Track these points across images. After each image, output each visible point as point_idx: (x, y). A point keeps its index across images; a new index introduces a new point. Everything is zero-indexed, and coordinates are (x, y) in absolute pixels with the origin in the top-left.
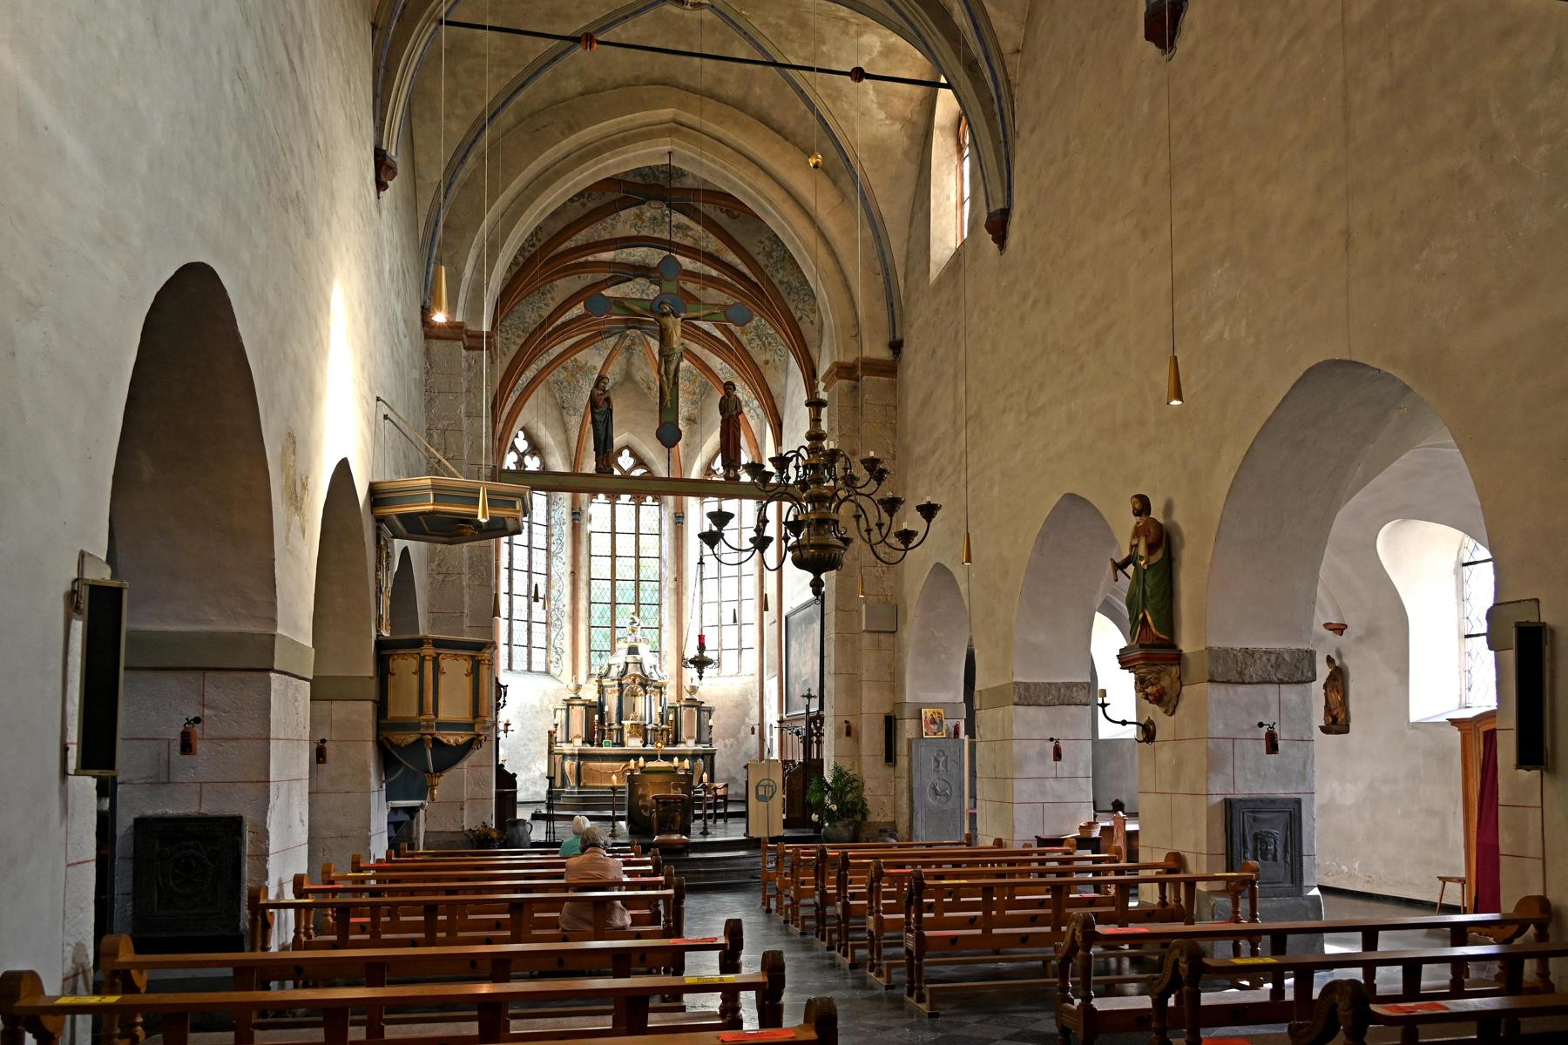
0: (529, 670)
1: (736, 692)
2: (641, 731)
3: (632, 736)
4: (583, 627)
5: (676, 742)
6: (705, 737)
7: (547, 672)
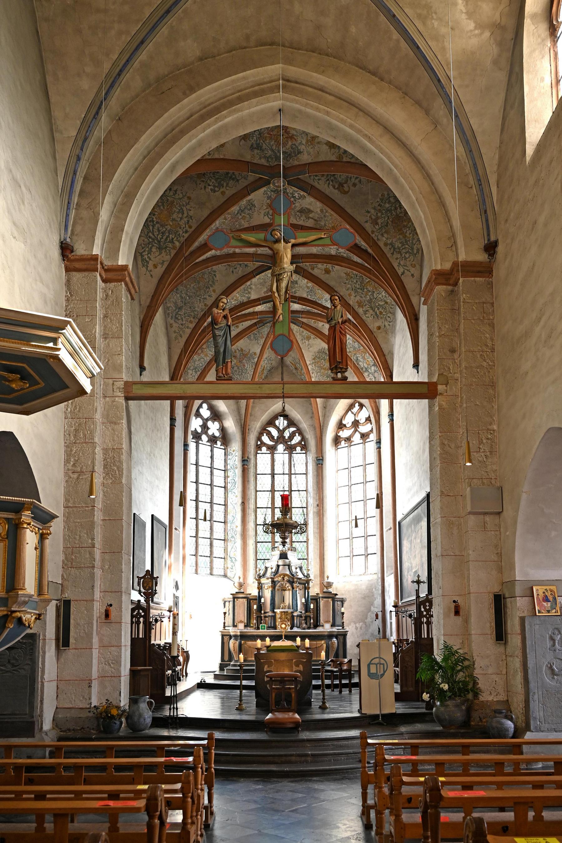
1: (364, 587)
4: (251, 543)
5: (316, 626)
6: (338, 621)
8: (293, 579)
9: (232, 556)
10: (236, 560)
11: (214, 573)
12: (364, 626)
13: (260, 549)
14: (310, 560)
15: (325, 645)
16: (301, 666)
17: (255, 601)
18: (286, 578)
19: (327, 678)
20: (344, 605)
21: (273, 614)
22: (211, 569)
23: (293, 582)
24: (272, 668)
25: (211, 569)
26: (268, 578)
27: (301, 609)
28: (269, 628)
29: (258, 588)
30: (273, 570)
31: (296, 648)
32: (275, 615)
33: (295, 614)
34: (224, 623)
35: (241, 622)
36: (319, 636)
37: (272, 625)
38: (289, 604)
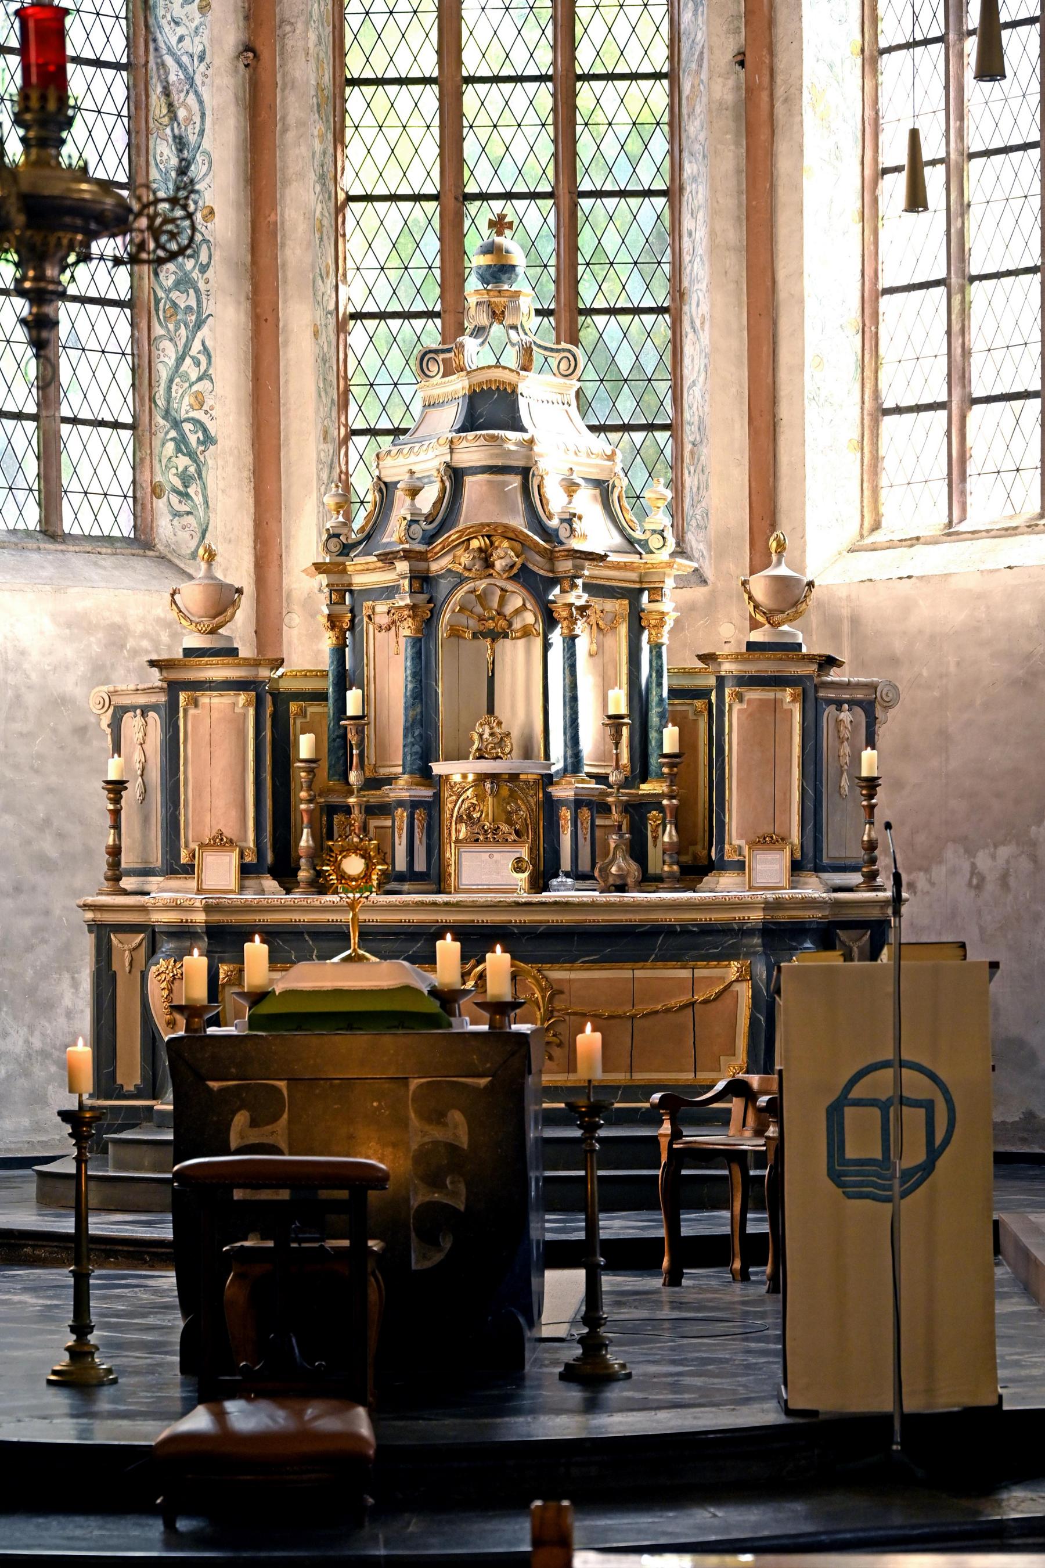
0: (50, 530)
2: (530, 811)
3: (484, 836)
4: (299, 320)
6: (844, 837)
7: (142, 541)
8: (551, 557)
9: (184, 408)
10: (208, 439)
11: (68, 525)
12: (1025, 864)
13: (371, 362)
14: (690, 434)
15: (745, 991)
16: (457, 1116)
17: (313, 709)
18: (504, 556)
19: (630, 1197)
20: (883, 732)
21: (426, 793)
22: (50, 494)
23: (553, 582)
24: (279, 1131)
25: (50, 494)
26: (388, 559)
27: (602, 757)
28: (391, 881)
29: (333, 621)
30: (426, 501)
31: (434, 1006)
32: (437, 796)
33: (564, 792)
34: (115, 852)
35: (220, 843)
36: (708, 930)
37: (420, 866)
38: (529, 724)
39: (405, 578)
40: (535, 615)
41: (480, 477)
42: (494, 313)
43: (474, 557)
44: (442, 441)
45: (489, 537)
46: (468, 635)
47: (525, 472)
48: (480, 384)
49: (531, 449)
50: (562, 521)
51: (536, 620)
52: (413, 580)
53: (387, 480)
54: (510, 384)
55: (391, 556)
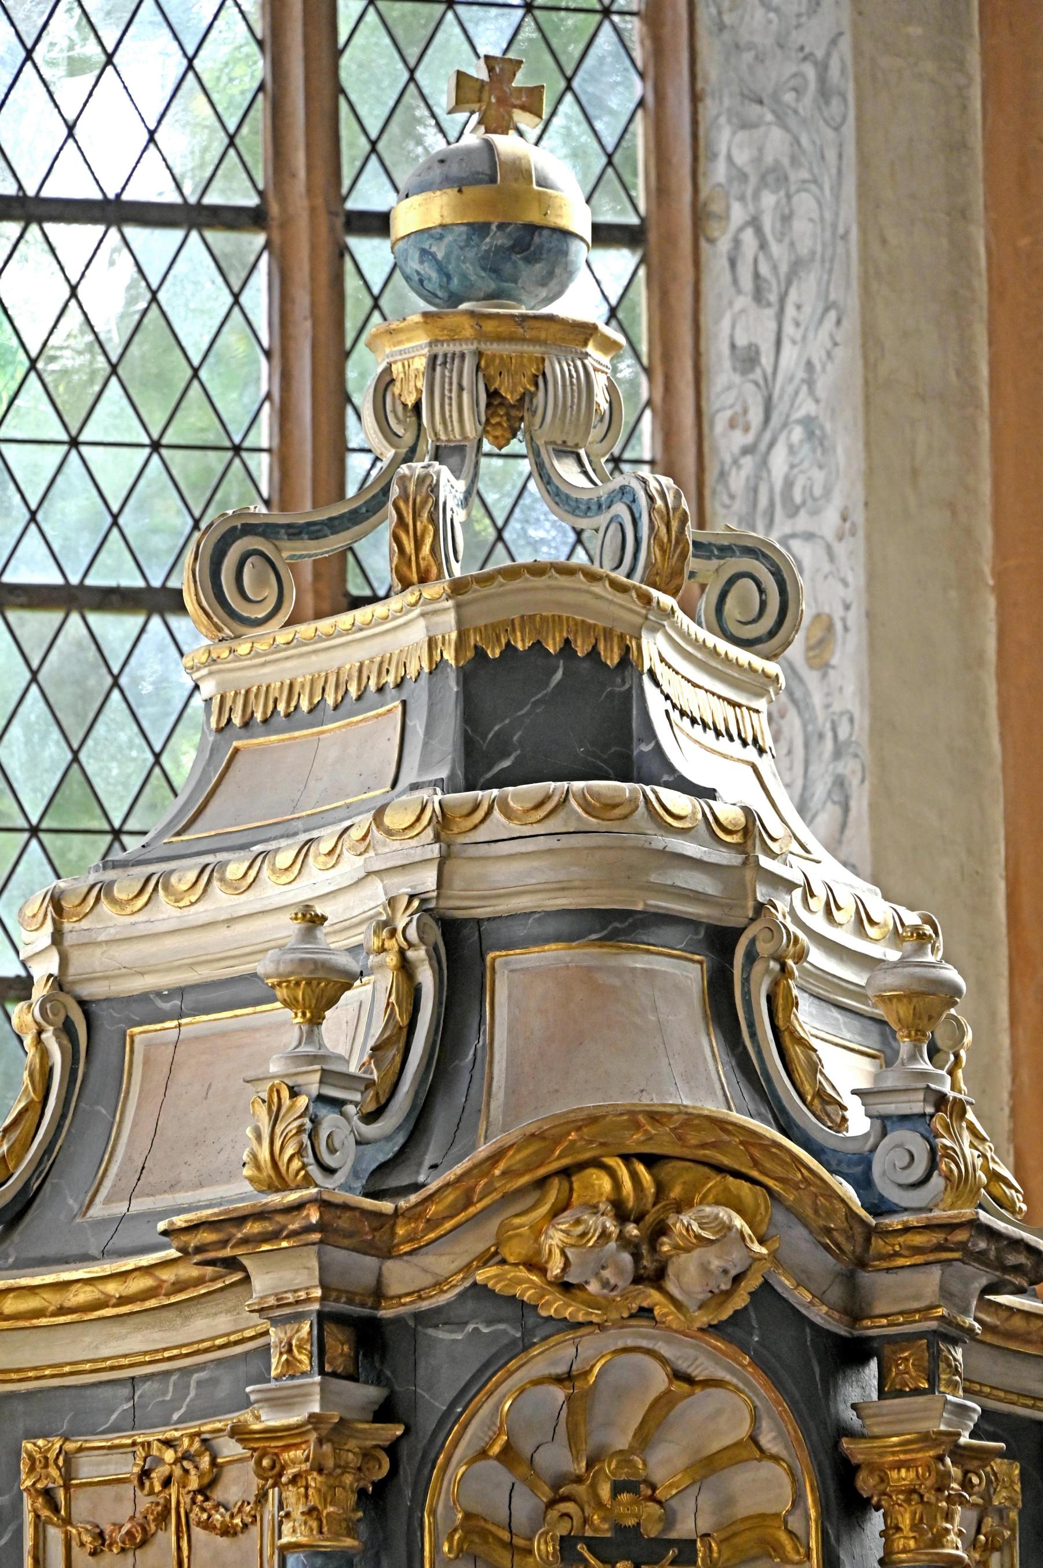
39: (298, 1317)
40: (792, 1473)
41: (552, 953)
42: (493, 395)
43: (604, 1235)
44: (394, 819)
45: (651, 1161)
46: (544, 1547)
47: (719, 943)
48: (493, 630)
49: (750, 861)
50: (884, 1123)
51: (798, 1499)
52: (330, 1328)
53: (87, 991)
54: (608, 633)
55: (253, 1228)
